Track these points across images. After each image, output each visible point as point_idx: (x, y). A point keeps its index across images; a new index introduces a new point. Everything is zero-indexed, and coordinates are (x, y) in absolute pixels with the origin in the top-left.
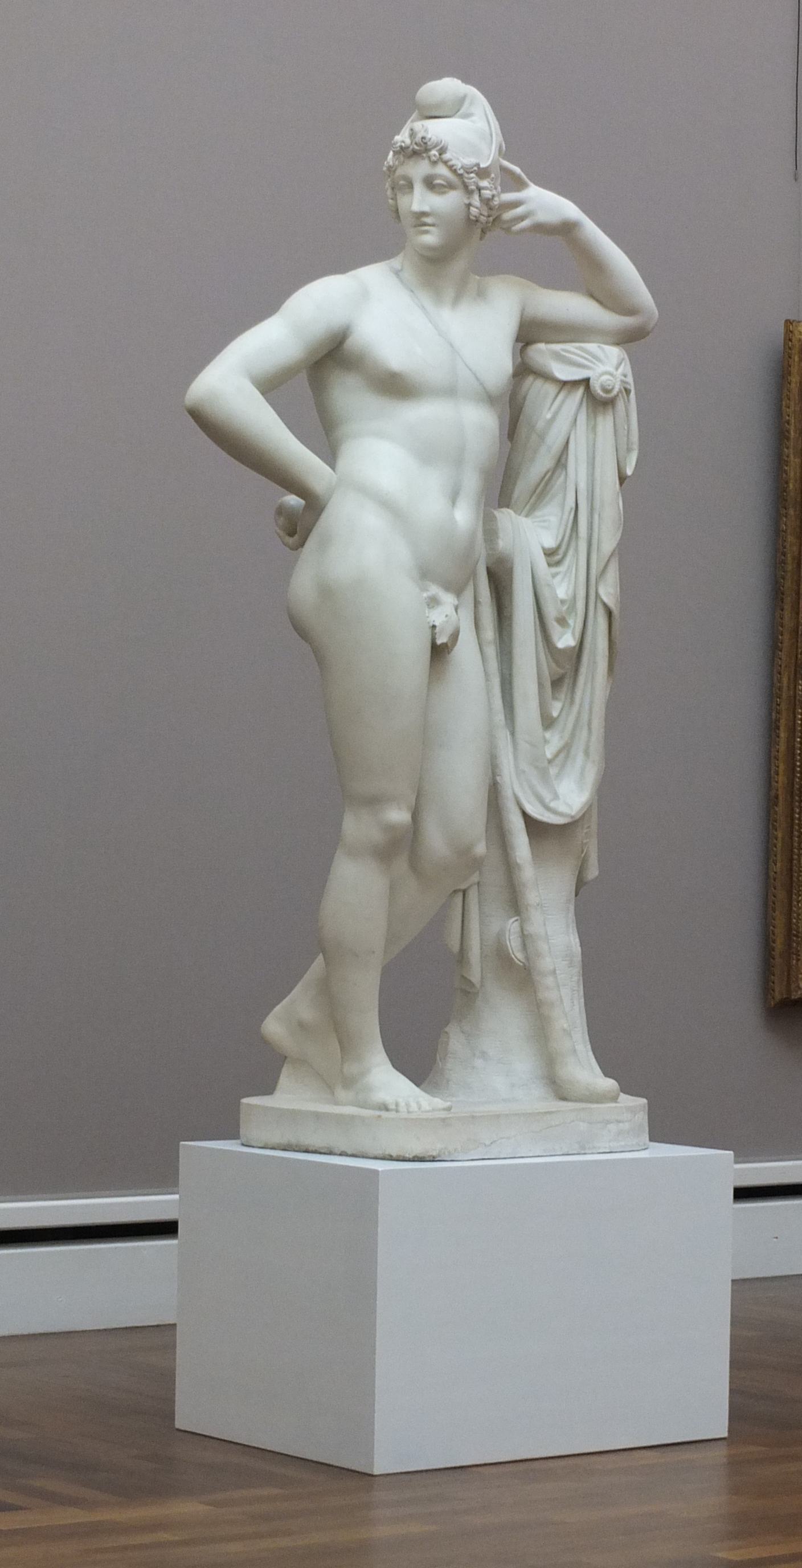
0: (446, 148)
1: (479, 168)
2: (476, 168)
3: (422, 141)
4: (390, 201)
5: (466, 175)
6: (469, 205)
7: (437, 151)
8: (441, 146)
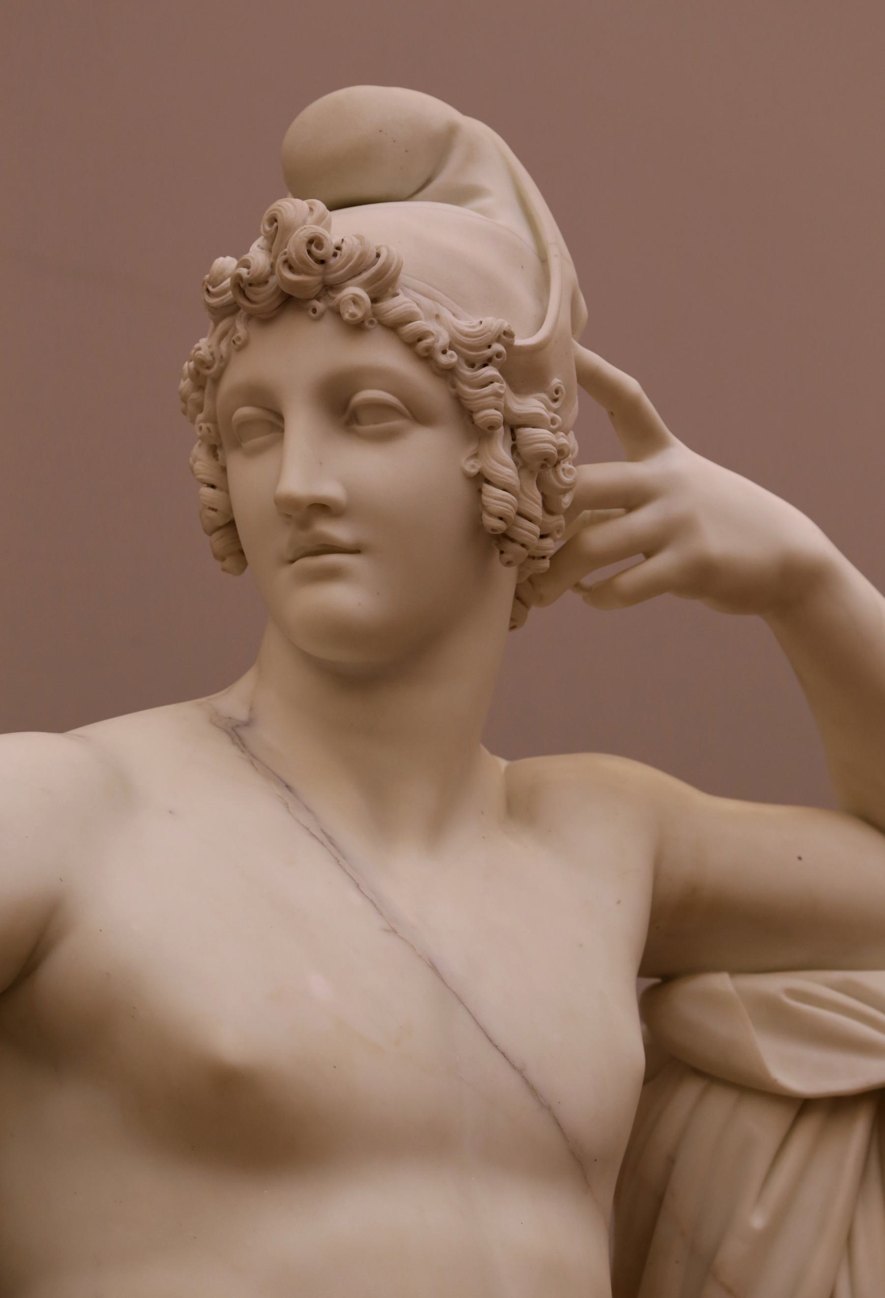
0: (393, 280)
1: (509, 346)
2: (498, 347)
3: (309, 252)
4: (206, 491)
5: (467, 372)
6: (480, 480)
7: (364, 285)
8: (373, 270)
